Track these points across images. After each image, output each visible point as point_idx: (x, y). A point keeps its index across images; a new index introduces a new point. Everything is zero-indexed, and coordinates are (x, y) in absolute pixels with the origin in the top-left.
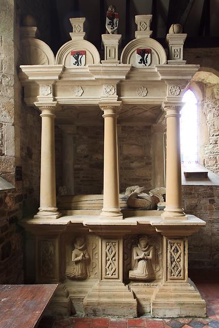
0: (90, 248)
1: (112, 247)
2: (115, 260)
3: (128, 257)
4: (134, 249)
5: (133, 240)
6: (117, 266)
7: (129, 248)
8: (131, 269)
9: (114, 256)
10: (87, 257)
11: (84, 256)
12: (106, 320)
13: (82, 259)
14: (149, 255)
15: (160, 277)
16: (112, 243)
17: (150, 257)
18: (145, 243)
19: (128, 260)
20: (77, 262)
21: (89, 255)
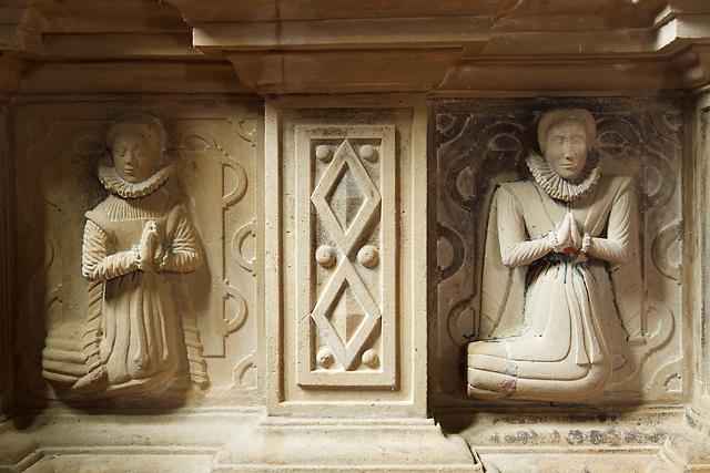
0: (207, 199)
1: (356, 174)
2: (373, 264)
3: (458, 253)
4: (502, 192)
5: (491, 145)
6: (385, 306)
7: (466, 193)
8: (477, 335)
9: (367, 236)
10: (184, 252)
11: (163, 241)
12: (500, 147)
13: (152, 262)
14: (604, 234)
15: (676, 388)
16: (356, 143)
17: (615, 241)
18: (581, 147)
19: (460, 274)
20: (117, 286)
21: (199, 244)
